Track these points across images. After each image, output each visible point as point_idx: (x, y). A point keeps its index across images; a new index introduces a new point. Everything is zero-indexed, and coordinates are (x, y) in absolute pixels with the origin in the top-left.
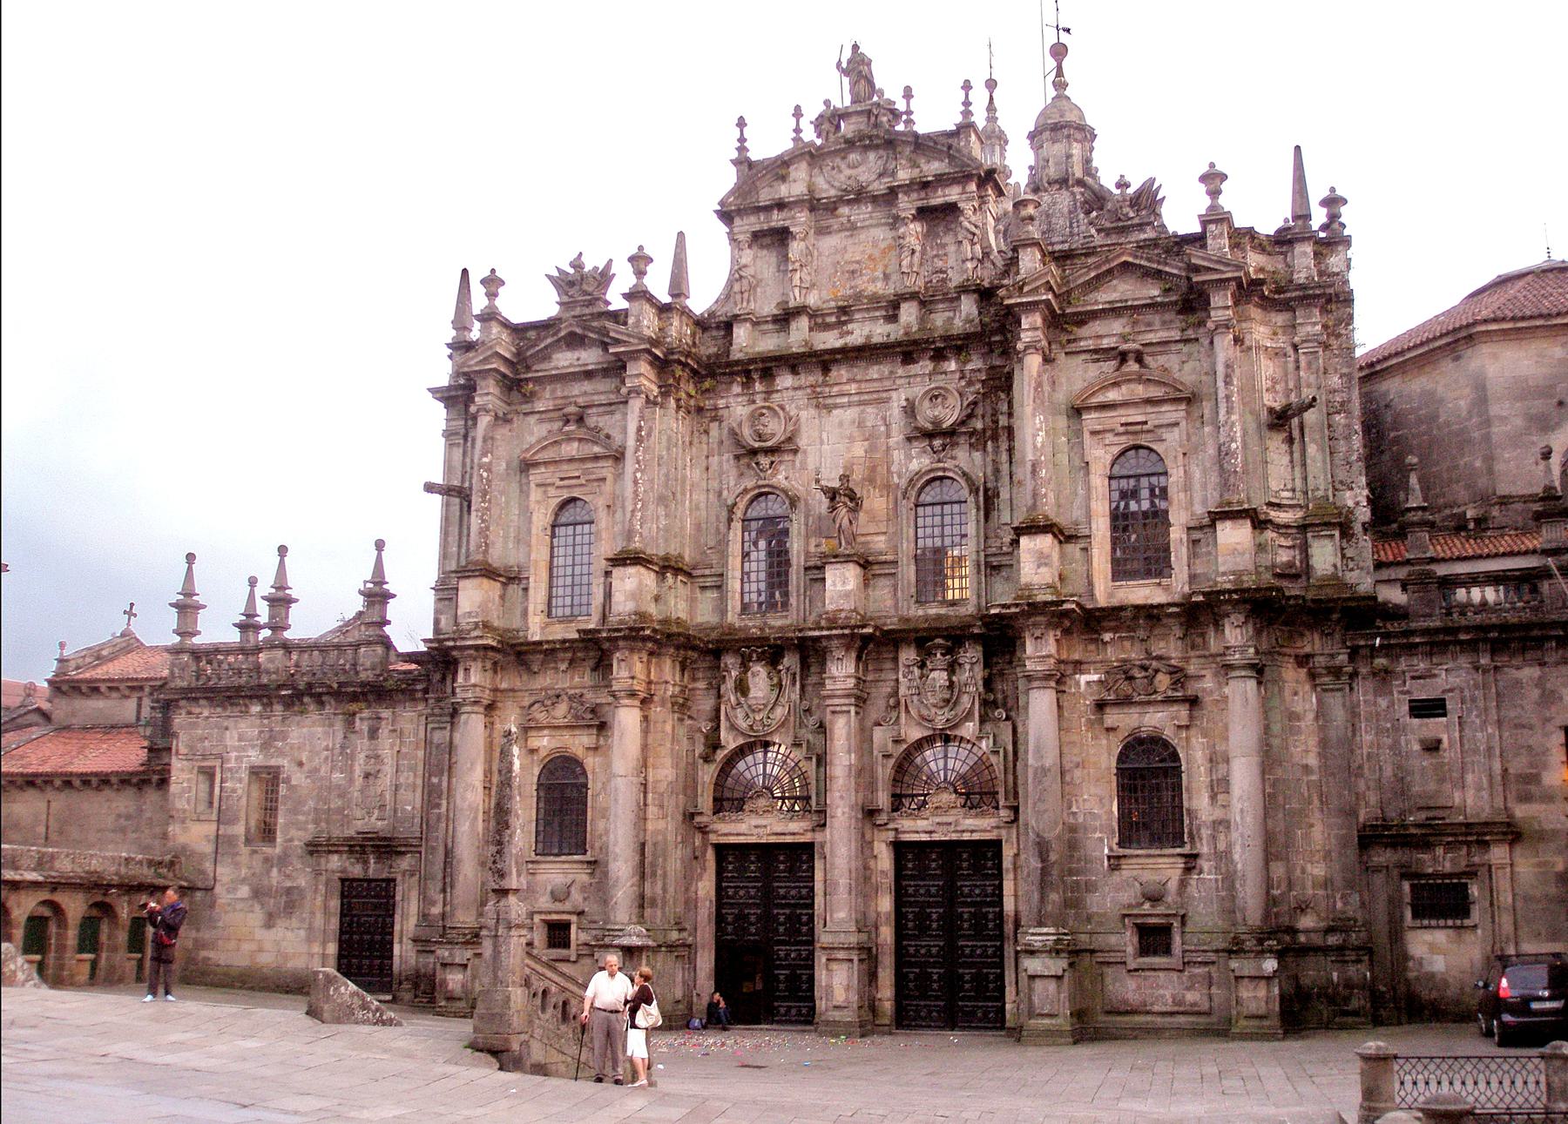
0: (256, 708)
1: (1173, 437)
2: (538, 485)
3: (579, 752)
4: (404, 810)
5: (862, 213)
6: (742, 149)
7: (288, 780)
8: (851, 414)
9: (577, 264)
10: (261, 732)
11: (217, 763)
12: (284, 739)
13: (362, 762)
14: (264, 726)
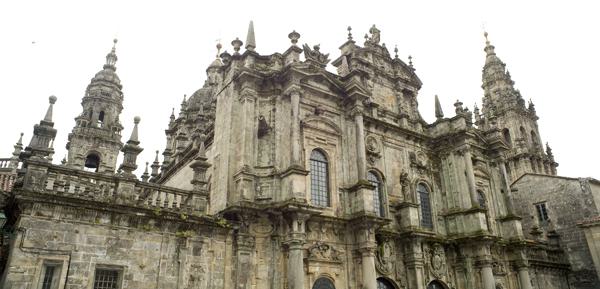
0: (105, 220)
3: (334, 276)
5: (385, 81)
7: (129, 278)
9: (317, 48)
11: (66, 259)
14: (112, 234)
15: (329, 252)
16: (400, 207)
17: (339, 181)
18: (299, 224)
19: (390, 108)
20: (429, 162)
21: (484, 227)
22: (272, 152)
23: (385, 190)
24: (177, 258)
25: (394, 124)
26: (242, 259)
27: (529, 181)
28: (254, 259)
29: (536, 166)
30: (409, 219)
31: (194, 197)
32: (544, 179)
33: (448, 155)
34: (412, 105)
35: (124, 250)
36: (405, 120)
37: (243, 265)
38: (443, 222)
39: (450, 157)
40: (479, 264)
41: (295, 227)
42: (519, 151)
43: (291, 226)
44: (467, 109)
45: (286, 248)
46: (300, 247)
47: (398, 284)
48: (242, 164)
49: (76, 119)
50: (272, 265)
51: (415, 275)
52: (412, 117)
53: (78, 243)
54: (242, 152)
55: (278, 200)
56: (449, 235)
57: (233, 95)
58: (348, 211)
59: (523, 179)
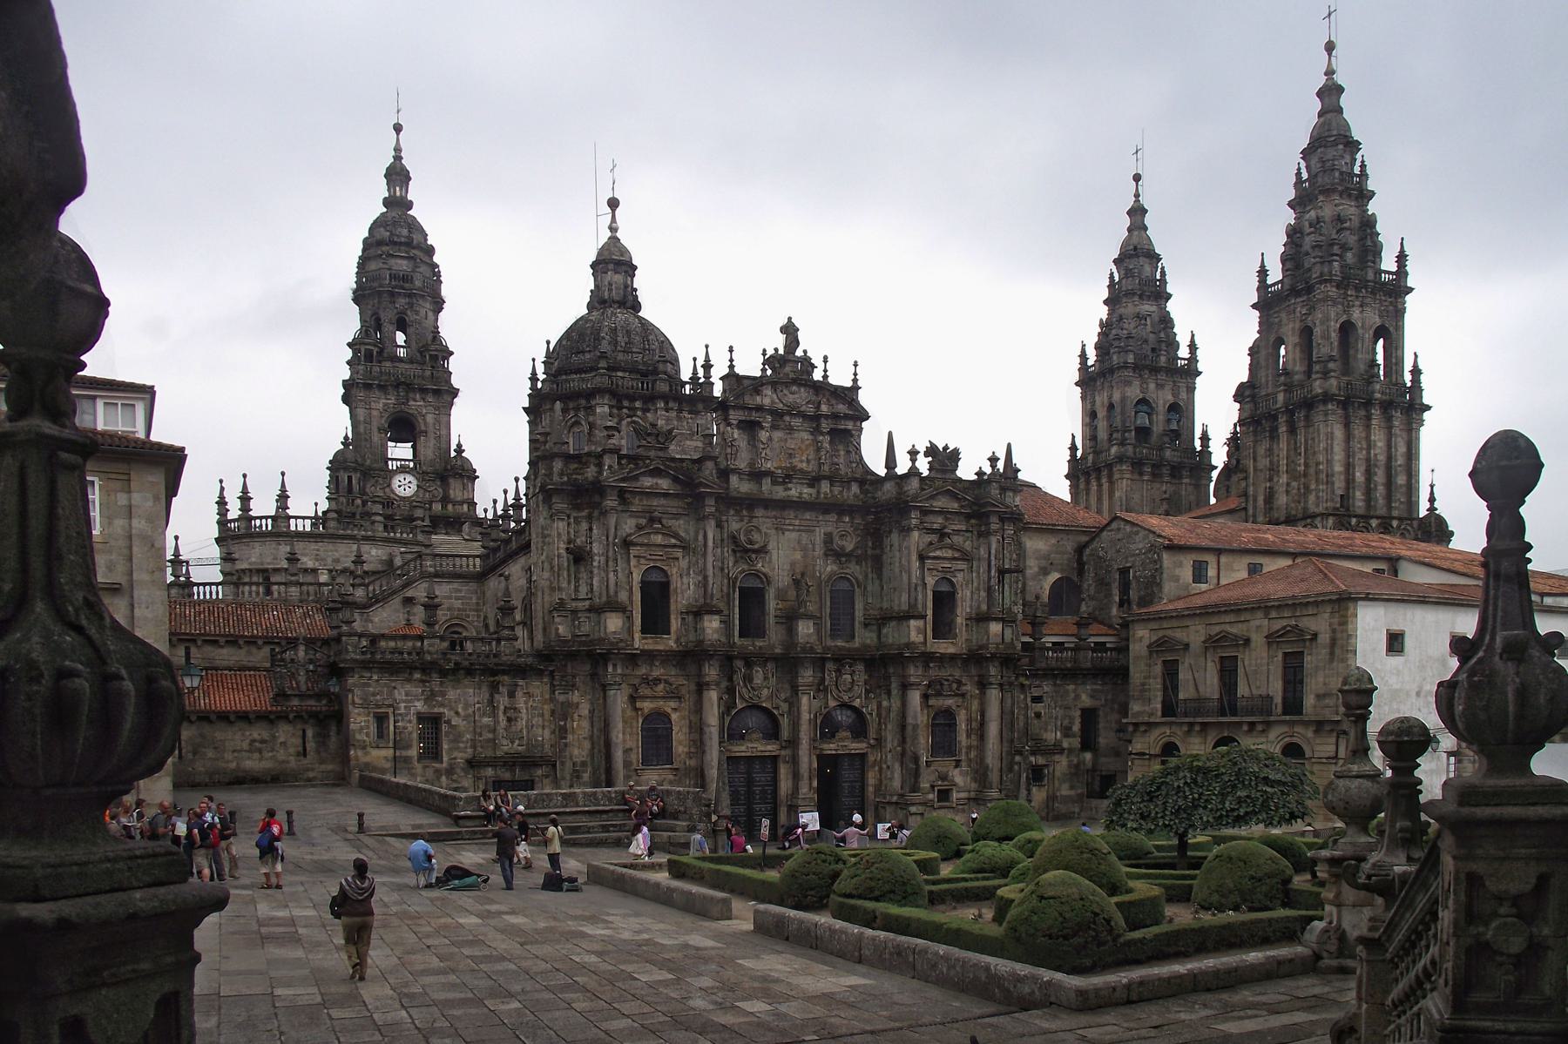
1: (960, 576)
3: (669, 710)
4: (536, 740)
5: (796, 422)
6: (731, 367)
7: (448, 722)
8: (794, 535)
18: (615, 666)
24: (491, 701)
27: (1119, 529)
28: (575, 697)
33: (890, 532)
34: (848, 452)
37: (562, 703)
40: (905, 687)
43: (606, 666)
45: (604, 688)
49: (349, 345)
50: (592, 704)
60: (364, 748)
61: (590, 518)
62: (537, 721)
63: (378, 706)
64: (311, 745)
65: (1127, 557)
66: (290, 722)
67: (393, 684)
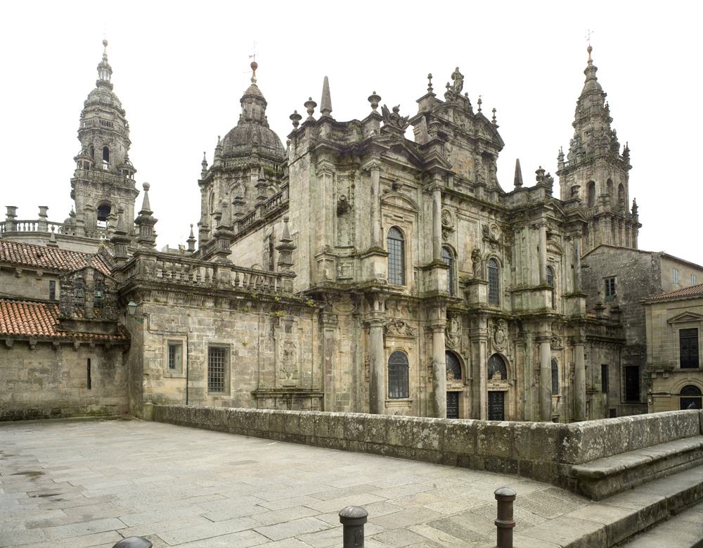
0: (210, 304)
2: (384, 215)
3: (407, 350)
4: (307, 374)
7: (236, 353)
10: (215, 321)
11: (184, 339)
12: (232, 327)
13: (282, 345)
15: (404, 328)
16: (469, 283)
17: (414, 260)
18: (380, 304)
19: (466, 175)
20: (502, 235)
21: (549, 305)
22: (351, 231)
23: (457, 266)
24: (272, 335)
25: (470, 194)
26: (327, 335)
27: (603, 253)
28: (338, 335)
29: (617, 228)
30: (477, 296)
31: (283, 279)
32: (619, 252)
33: (523, 228)
34: (490, 171)
35: (229, 330)
36: (481, 190)
37: (328, 340)
38: (509, 298)
39: (524, 231)
40: (539, 340)
41: (377, 307)
42: (601, 209)
44: (548, 176)
45: (367, 326)
46: (380, 325)
47: (462, 356)
48: (322, 243)
50: (354, 340)
51: (478, 349)
52: (489, 184)
53: (192, 326)
54: (322, 232)
55: (358, 281)
56: (514, 311)
57: (310, 169)
58: (421, 289)
59: (597, 251)
60: (158, 378)
61: (352, 177)
62: (308, 356)
63: (172, 334)
64: (96, 376)
65: (612, 270)
66: (75, 350)
67: (188, 312)
